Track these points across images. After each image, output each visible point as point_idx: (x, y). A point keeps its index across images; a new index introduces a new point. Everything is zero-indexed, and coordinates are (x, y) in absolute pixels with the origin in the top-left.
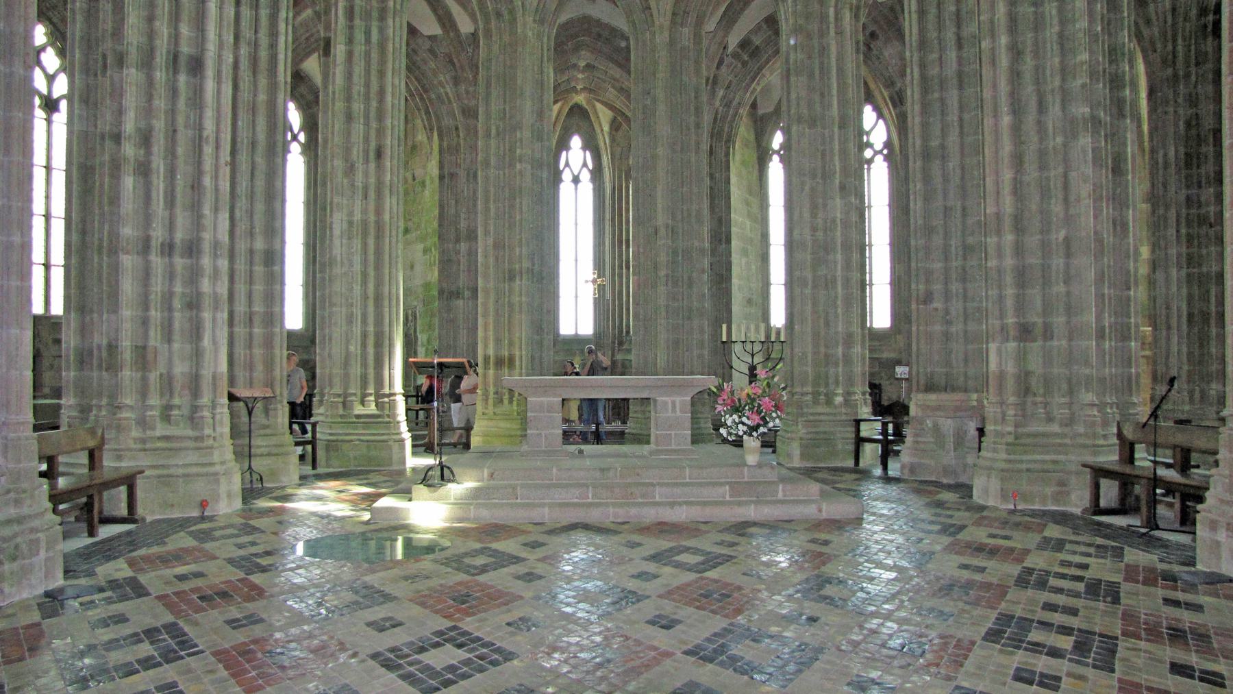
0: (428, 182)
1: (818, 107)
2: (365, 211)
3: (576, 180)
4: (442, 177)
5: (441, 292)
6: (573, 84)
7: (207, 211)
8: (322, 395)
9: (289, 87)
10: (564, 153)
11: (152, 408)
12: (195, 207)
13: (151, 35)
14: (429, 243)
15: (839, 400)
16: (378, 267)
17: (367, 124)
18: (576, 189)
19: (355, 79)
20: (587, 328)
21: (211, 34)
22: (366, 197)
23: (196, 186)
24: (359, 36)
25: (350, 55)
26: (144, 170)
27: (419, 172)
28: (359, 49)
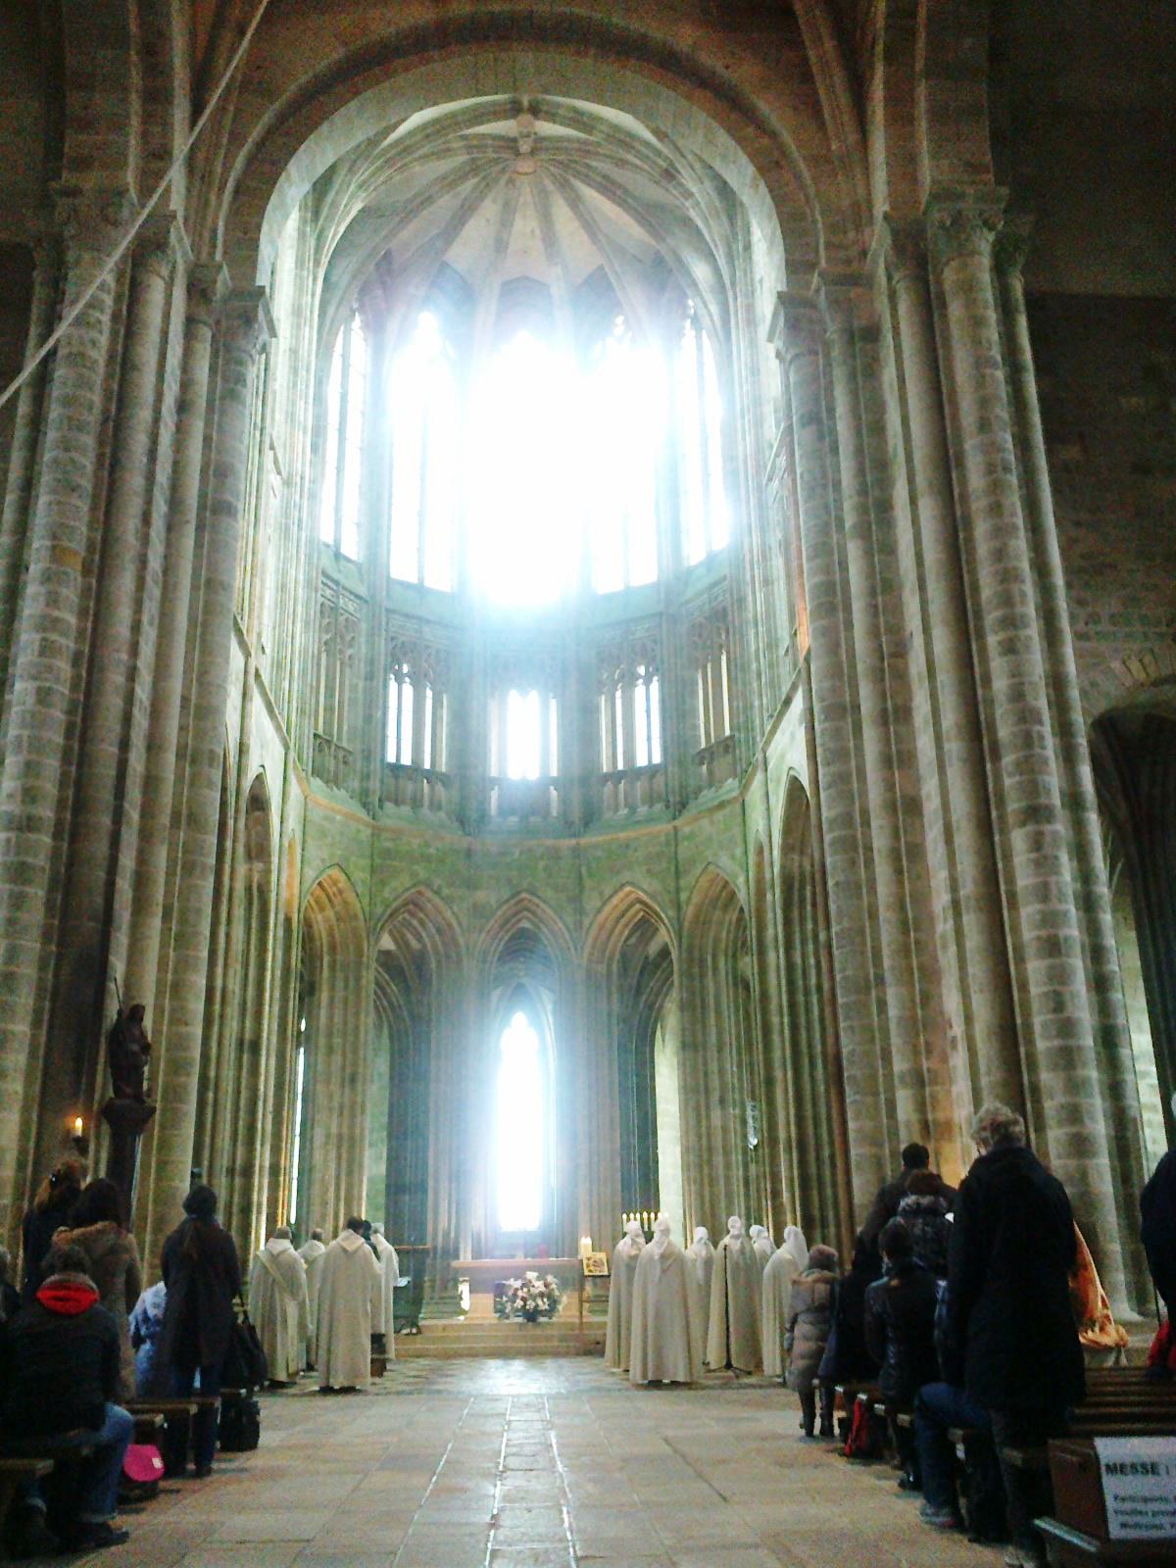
1: (700, 1034)
2: (340, 1126)
4: (392, 1078)
5: (388, 1186)
7: (258, 1147)
12: (250, 1143)
16: (350, 1173)
17: (344, 1055)
19: (336, 1020)
21: (265, 1027)
22: (341, 1115)
23: (251, 1128)
24: (340, 984)
25: (332, 1000)
28: (339, 995)
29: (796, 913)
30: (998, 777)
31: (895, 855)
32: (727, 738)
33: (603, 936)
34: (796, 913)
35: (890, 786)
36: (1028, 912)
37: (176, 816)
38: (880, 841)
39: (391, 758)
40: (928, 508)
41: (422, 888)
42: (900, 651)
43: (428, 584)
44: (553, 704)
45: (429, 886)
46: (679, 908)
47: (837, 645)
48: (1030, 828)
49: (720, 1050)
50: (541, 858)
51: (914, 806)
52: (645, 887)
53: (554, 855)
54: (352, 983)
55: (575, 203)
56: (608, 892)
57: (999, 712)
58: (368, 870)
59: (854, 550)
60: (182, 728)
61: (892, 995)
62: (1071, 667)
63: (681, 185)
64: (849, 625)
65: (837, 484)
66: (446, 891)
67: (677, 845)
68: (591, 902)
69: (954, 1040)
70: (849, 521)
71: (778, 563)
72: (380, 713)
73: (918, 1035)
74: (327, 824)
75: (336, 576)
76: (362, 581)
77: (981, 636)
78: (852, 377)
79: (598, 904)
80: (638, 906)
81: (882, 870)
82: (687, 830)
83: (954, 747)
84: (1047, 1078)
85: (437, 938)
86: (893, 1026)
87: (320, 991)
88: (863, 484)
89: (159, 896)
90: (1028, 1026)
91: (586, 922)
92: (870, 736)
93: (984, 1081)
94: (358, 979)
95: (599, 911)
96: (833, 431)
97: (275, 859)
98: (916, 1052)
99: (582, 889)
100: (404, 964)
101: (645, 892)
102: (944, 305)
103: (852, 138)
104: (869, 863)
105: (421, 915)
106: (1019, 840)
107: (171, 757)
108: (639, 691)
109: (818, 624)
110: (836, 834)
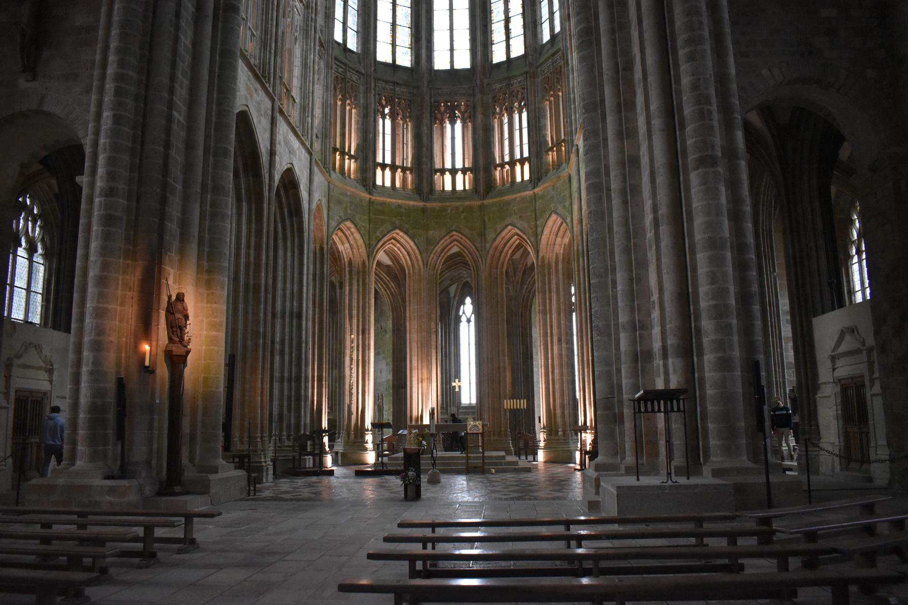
0: (388, 331)
3: (469, 321)
6: (462, 275)
8: (339, 433)
9: (328, 311)
10: (462, 306)
11: (284, 435)
13: (284, 306)
14: (388, 361)
15: (560, 433)
18: (469, 326)
20: (474, 401)
21: (304, 305)
26: (282, 353)
27: (383, 324)
28: (355, 287)
30: (683, 141)
31: (623, 192)
33: (497, 254)
35: (621, 150)
36: (699, 221)
37: (204, 186)
38: (615, 184)
39: (380, 160)
41: (398, 231)
43: (398, 63)
47: (593, 66)
49: (559, 313)
50: (463, 212)
52: (518, 226)
53: (470, 209)
54: (361, 284)
56: (499, 229)
58: (367, 222)
60: (207, 137)
61: (620, 277)
67: (535, 202)
68: (490, 236)
69: (654, 302)
72: (371, 135)
73: (633, 301)
74: (341, 197)
75: (344, 60)
76: (360, 63)
77: (675, 52)
79: (493, 236)
81: (616, 202)
82: (540, 193)
83: (657, 123)
84: (707, 324)
87: (345, 287)
89: (195, 230)
90: (696, 293)
91: (488, 246)
92: (610, 119)
93: (668, 326)
94: (364, 280)
95: (495, 240)
97: (306, 216)
98: (632, 310)
99: (485, 229)
100: (397, 273)
101: (519, 229)
104: (609, 198)
106: (694, 178)
107: (200, 152)
108: (517, 117)
109: (581, 54)
110: (590, 182)
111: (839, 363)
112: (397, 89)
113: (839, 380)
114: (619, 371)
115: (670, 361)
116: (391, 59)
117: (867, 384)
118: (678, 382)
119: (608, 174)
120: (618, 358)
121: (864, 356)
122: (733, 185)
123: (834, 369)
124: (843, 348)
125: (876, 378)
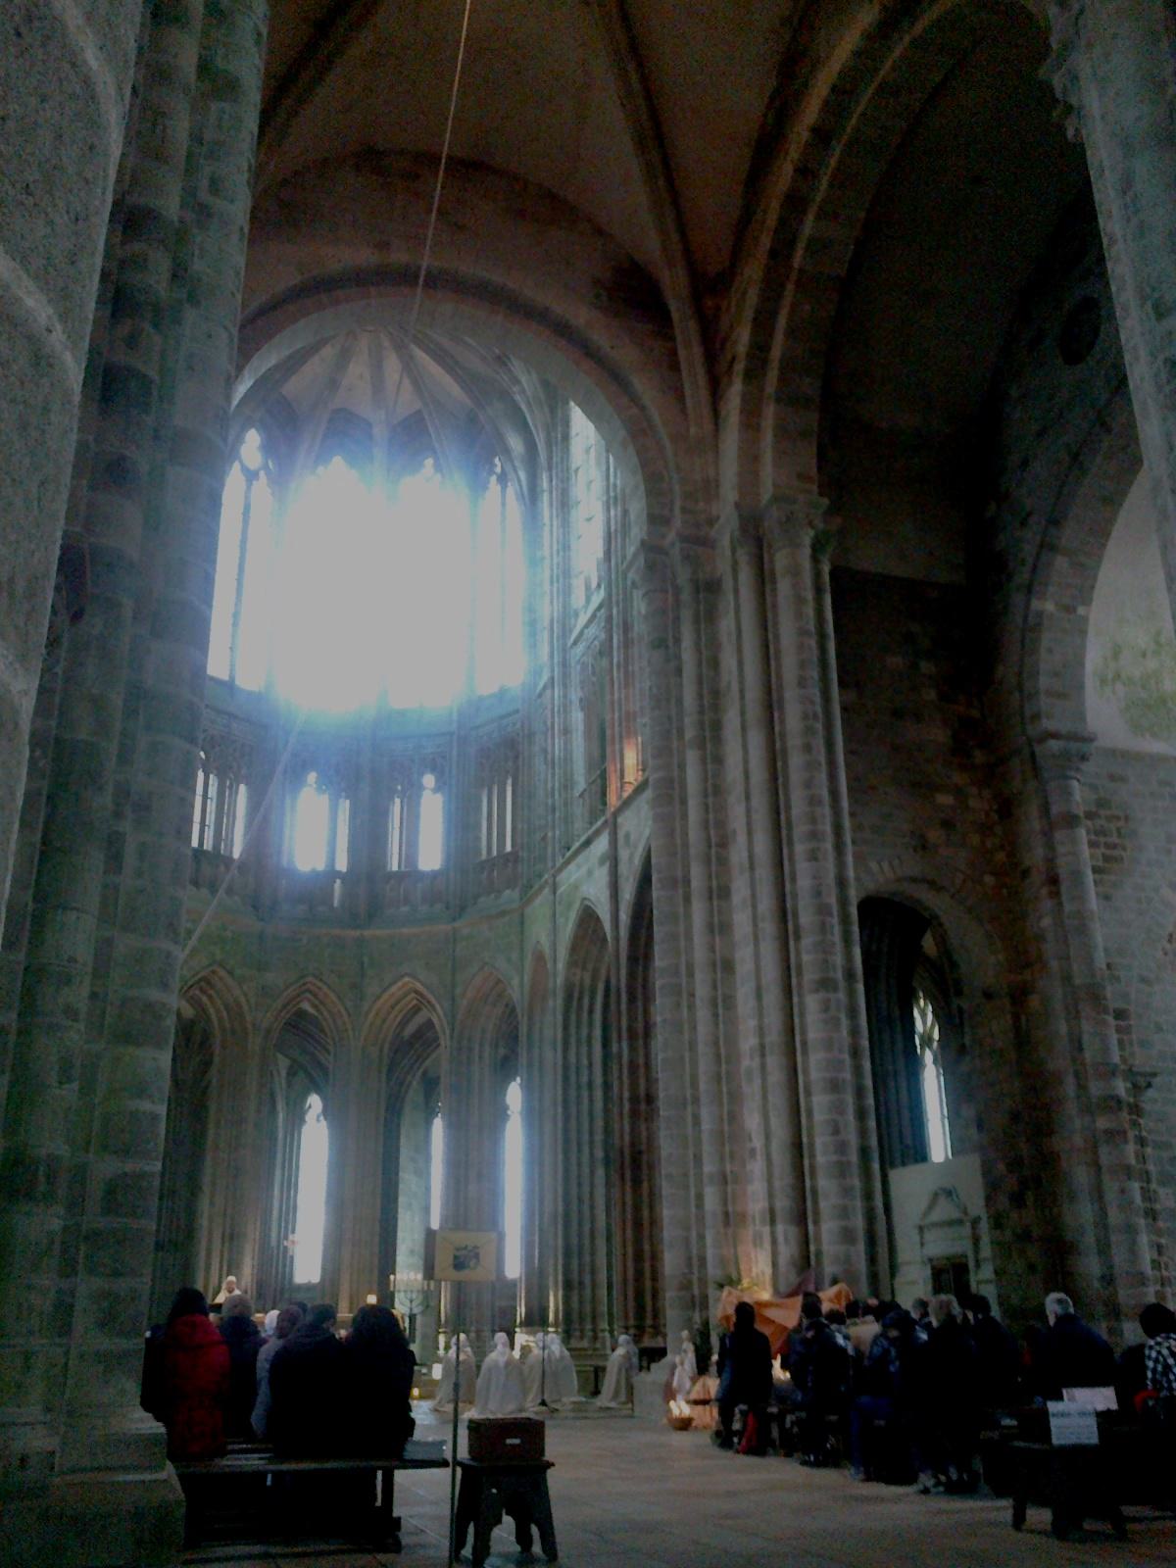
29: (573, 1017)
32: (509, 854)
34: (573, 1017)
35: (712, 949)
38: (702, 991)
39: (195, 843)
40: (756, 739)
41: (215, 967)
42: (724, 843)
43: (239, 682)
44: (345, 806)
45: (221, 965)
46: (453, 999)
47: (673, 831)
48: (822, 995)
51: (729, 966)
55: (409, 366)
57: (801, 904)
59: (692, 757)
61: (706, 1114)
62: (851, 873)
63: (510, 370)
64: (685, 816)
65: (680, 701)
66: (238, 972)
69: (753, 1152)
70: (690, 733)
71: (578, 717)
78: (697, 621)
80: (413, 995)
81: (703, 1014)
83: (769, 928)
85: (225, 1014)
86: (705, 1137)
88: (701, 706)
90: (812, 1145)
92: (698, 909)
93: (777, 1184)
95: (379, 997)
96: (678, 657)
102: (774, 582)
103: (709, 427)
104: (691, 1007)
105: (211, 992)
111: (929, 1236)
112: (235, 725)
113: (931, 1260)
114: (701, 1237)
115: (780, 1228)
116: (228, 673)
117: (971, 1264)
118: (792, 1256)
119: (691, 975)
120: (701, 1219)
121: (967, 1230)
122: (853, 1013)
123: (922, 1244)
124: (936, 1216)
125: (985, 1259)
